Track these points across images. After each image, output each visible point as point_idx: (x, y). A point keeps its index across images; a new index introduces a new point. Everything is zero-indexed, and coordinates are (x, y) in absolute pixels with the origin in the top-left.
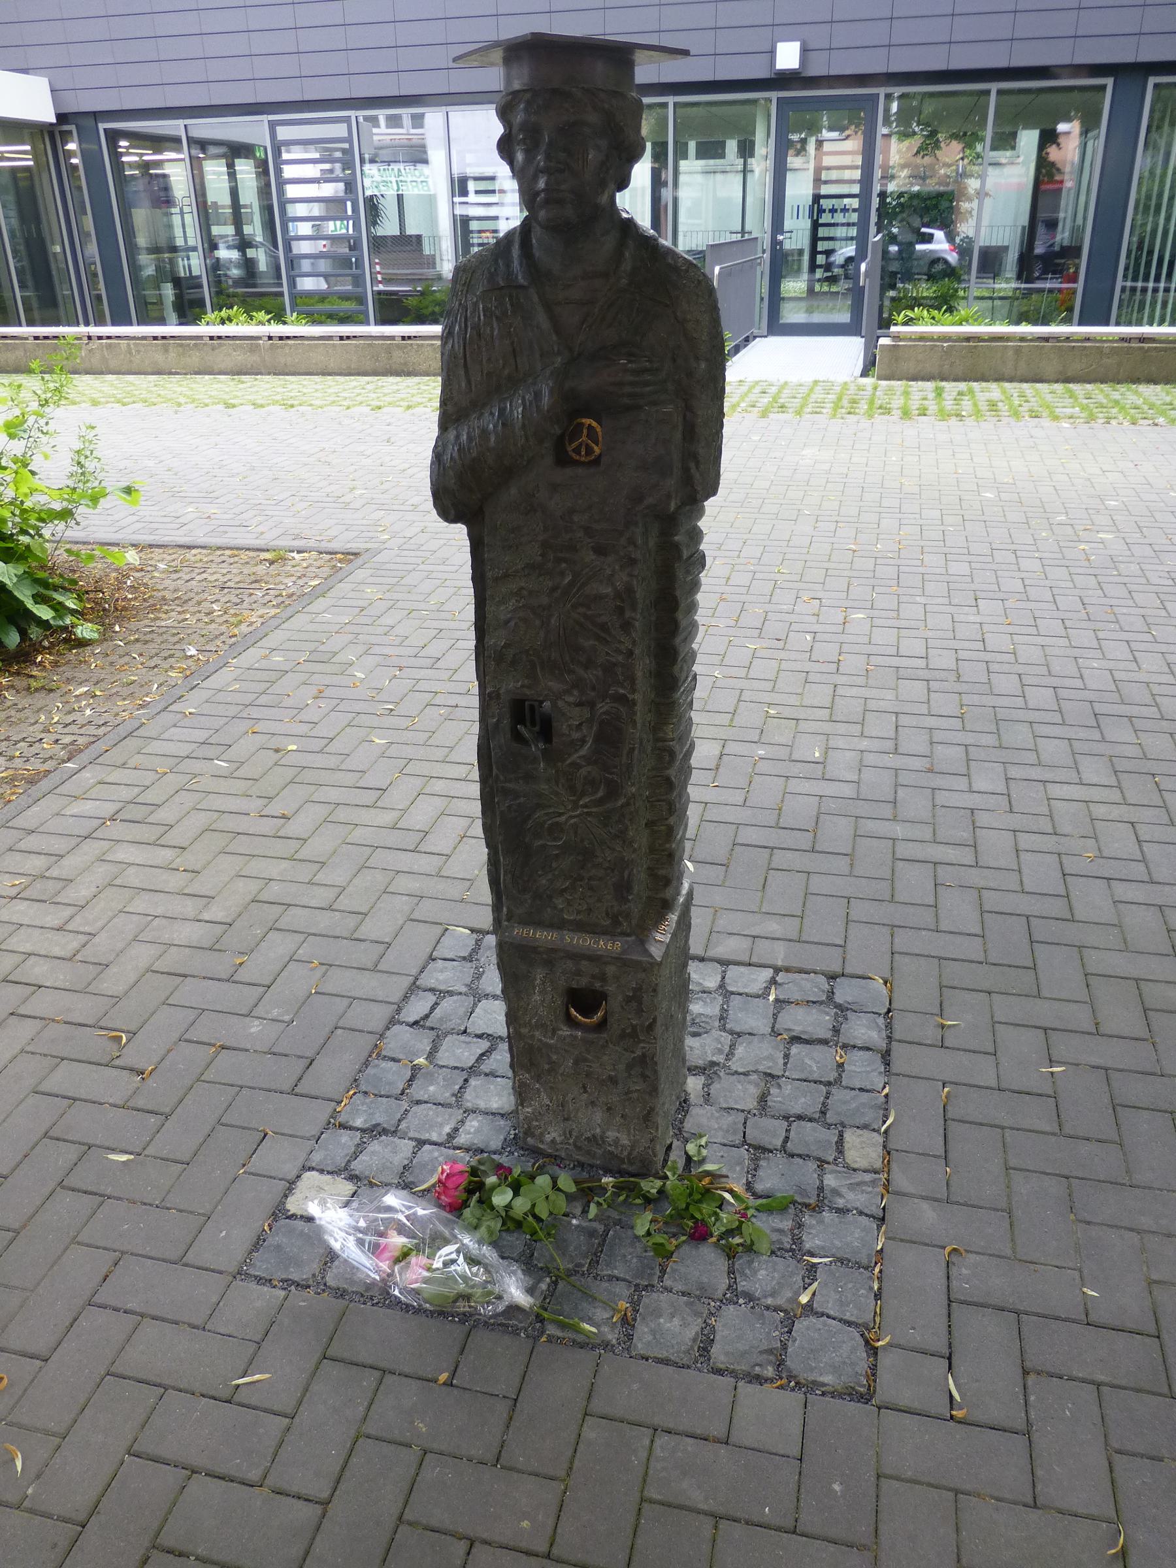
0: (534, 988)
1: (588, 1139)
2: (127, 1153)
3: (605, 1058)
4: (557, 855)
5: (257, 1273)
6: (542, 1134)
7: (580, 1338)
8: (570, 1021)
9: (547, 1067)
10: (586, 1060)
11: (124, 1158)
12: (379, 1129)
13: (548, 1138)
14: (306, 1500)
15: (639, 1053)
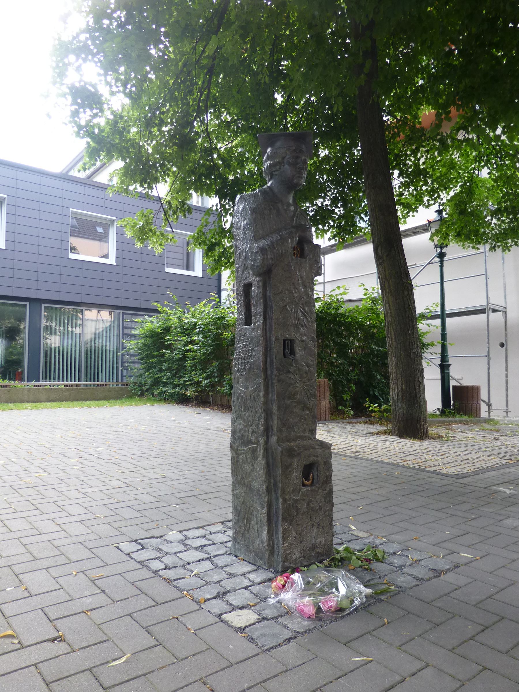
0: (293, 469)
1: (310, 548)
2: (120, 658)
3: (317, 497)
4: (295, 406)
5: (271, 646)
6: (291, 558)
7: (392, 594)
8: (304, 485)
9: (295, 513)
10: (311, 501)
11: (124, 659)
12: (221, 593)
13: (294, 557)
14: (423, 669)
15: (328, 490)
